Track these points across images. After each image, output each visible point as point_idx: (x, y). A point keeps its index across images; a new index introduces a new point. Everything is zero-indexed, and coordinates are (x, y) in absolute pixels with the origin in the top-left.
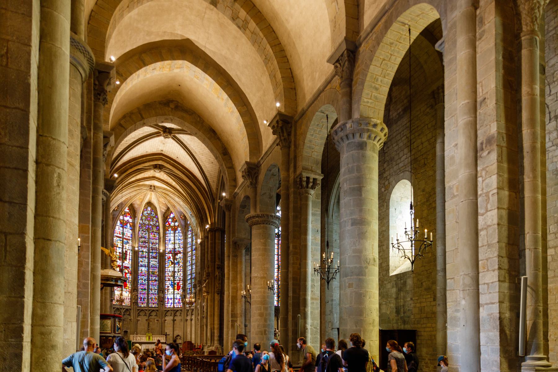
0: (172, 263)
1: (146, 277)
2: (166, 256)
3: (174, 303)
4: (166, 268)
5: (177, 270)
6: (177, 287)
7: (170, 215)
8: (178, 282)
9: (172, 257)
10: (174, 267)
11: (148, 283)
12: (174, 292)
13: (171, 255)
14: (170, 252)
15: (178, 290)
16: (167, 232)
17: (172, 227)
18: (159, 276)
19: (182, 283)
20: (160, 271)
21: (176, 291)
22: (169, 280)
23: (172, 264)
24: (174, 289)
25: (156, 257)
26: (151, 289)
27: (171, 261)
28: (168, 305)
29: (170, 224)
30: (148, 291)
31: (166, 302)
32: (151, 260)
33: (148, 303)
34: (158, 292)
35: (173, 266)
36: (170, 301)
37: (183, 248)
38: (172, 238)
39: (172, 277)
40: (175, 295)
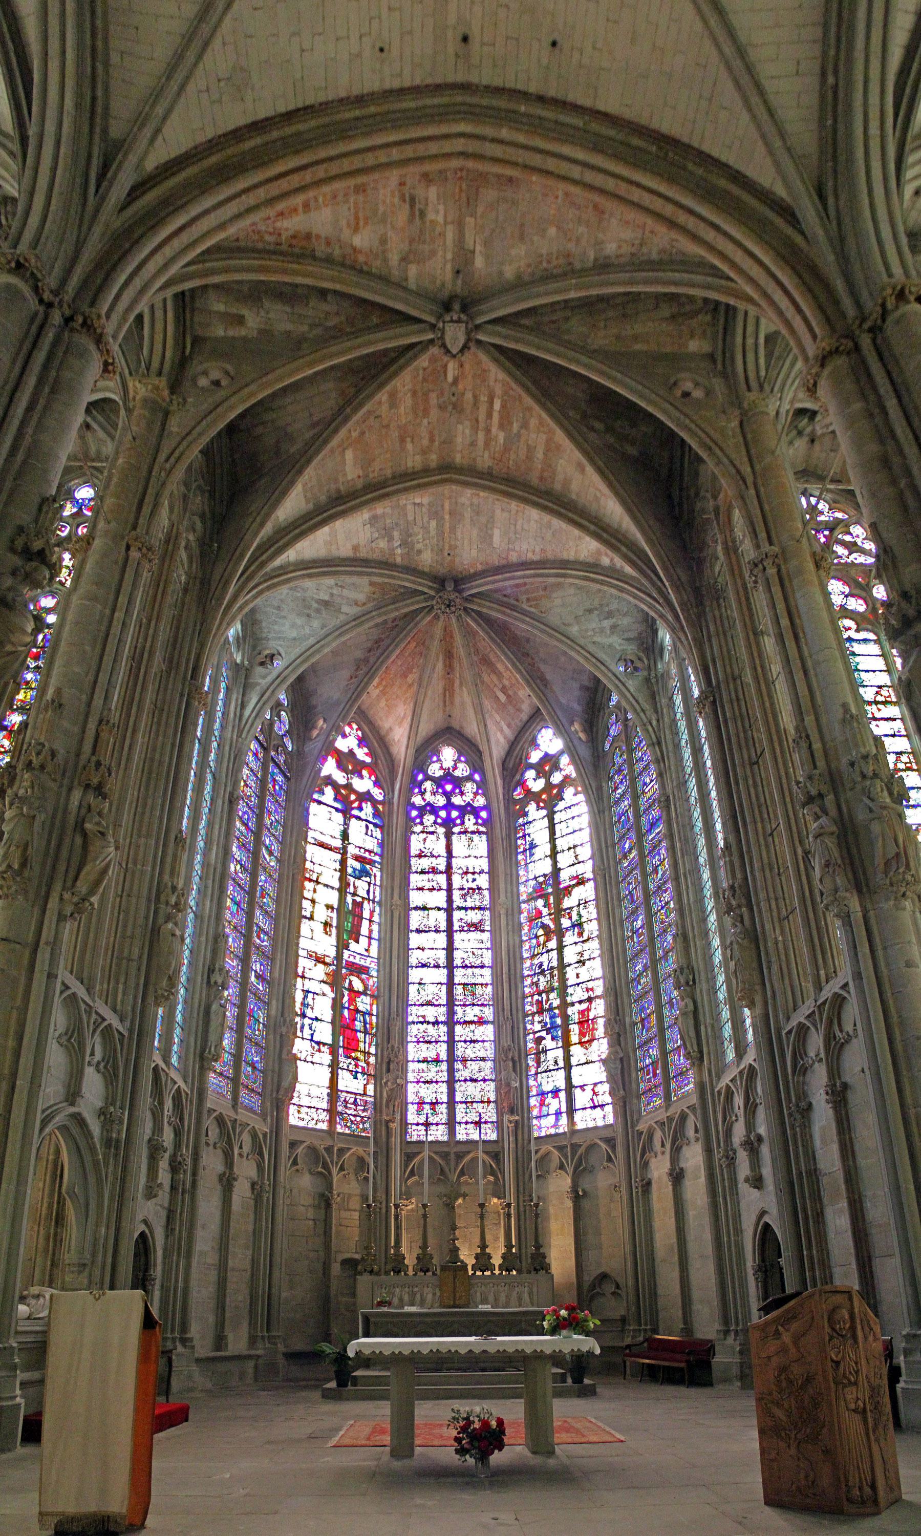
11: (451, 1033)
18: (497, 1002)
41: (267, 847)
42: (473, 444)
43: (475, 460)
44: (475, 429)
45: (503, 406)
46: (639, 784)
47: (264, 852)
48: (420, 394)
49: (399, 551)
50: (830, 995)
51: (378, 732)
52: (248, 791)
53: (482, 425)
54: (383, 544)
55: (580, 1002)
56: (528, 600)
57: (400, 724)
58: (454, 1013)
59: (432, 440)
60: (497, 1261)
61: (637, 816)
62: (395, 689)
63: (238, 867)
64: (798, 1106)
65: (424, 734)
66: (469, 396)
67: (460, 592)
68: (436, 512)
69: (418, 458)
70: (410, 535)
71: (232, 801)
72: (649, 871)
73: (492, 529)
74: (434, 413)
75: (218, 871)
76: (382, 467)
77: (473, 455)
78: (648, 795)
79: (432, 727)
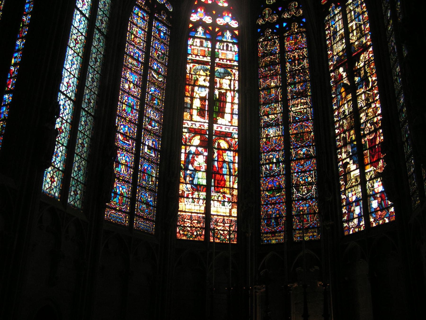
4: (333, 111)
6: (372, 156)
9: (344, 75)
11: (288, 168)
12: (363, 174)
13: (341, 70)
16: (326, 18)
21: (369, 169)
22: (345, 145)
23: (347, 94)
25: (305, 91)
27: (345, 85)
28: (351, 224)
30: (289, 194)
31: (345, 218)
32: (291, 103)
38: (339, 25)
39: (352, 132)
40: (368, 184)
52: (137, 40)
55: (369, 134)
58: (290, 154)
63: (132, 85)
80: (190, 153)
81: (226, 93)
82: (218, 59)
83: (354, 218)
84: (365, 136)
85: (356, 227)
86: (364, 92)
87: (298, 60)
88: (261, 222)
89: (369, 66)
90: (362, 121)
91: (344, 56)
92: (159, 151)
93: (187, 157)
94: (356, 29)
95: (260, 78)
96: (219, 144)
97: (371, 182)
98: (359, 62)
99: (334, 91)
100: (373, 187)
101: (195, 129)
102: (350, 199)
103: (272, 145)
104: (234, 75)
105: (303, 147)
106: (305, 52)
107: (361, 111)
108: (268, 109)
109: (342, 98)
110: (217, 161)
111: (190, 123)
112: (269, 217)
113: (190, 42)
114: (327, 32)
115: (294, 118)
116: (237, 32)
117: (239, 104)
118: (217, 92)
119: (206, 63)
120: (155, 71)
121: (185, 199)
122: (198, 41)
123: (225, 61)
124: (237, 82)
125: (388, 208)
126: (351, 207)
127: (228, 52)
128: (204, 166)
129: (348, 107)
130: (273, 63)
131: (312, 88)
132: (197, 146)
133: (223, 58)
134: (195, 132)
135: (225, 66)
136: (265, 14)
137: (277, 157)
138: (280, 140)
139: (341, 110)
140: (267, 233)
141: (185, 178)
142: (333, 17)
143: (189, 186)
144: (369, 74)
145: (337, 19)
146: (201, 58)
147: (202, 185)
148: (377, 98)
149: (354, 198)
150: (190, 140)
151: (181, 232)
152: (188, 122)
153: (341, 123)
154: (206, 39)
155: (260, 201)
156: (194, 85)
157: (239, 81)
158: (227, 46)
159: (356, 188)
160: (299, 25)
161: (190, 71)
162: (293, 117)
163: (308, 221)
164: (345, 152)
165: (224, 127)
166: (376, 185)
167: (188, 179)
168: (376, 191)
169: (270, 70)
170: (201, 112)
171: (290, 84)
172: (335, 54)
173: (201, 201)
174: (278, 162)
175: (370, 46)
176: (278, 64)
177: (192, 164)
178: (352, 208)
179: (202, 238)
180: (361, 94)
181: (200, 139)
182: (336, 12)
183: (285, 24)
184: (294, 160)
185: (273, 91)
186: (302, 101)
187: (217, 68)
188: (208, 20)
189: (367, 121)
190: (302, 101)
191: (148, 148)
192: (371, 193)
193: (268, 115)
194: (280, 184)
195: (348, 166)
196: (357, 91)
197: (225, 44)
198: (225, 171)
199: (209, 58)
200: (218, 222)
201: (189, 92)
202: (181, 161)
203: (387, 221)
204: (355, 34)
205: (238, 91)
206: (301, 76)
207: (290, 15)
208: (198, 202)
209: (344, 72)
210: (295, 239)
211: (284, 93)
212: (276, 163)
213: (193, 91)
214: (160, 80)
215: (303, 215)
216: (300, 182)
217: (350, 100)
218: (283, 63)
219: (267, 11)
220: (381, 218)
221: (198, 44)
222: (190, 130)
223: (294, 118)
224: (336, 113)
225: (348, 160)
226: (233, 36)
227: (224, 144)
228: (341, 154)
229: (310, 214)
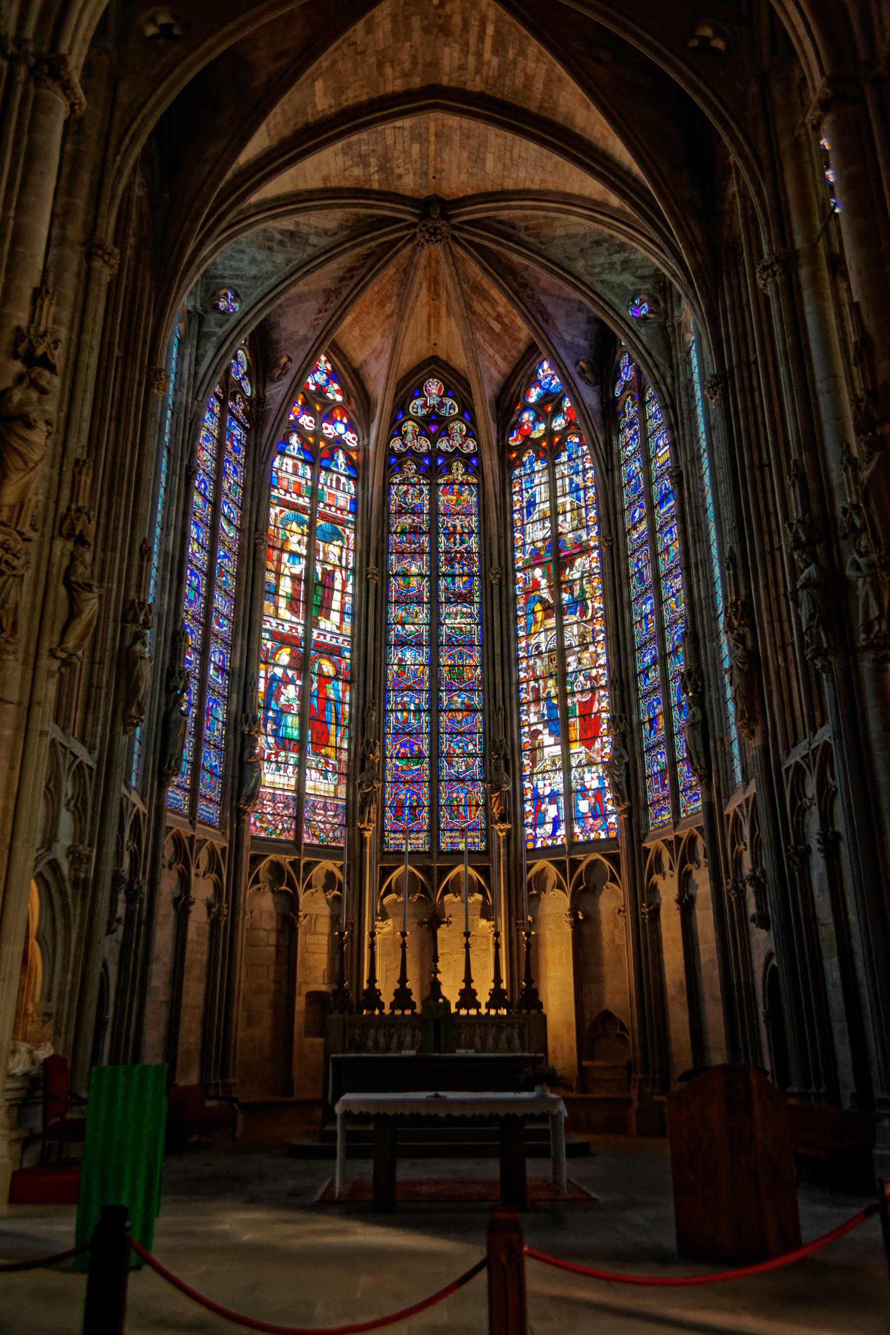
0: (548, 609)
1: (425, 695)
2: (515, 582)
3: (570, 821)
4: (517, 638)
5: (575, 641)
6: (583, 730)
7: (527, 394)
8: (586, 698)
9: (544, 583)
10: (561, 628)
11: (434, 724)
12: (566, 756)
14: (536, 560)
15: (588, 740)
16: (517, 472)
17: (538, 441)
19: (604, 704)
20: (488, 662)
21: (576, 748)
22: (537, 700)
23: (547, 617)
24: (566, 743)
25: (470, 592)
26: (449, 756)
27: (542, 601)
29: (527, 438)
30: (435, 769)
31: (530, 820)
32: (445, 609)
33: (434, 831)
34: (483, 766)
35: (552, 622)
36: (552, 811)
37: (598, 523)
38: (542, 493)
39: (551, 682)
41: (225, 516)
42: (462, 67)
43: (465, 83)
44: (465, 52)
45: (498, 31)
46: (652, 444)
47: (224, 523)
48: (400, 18)
49: (376, 177)
50: (821, 742)
51: (350, 364)
53: (472, 49)
54: (357, 171)
56: (526, 228)
57: (377, 357)
58: (440, 699)
59: (414, 62)
60: (483, 997)
61: (649, 483)
62: (371, 317)
64: (795, 848)
65: (405, 366)
66: (457, 19)
67: (447, 218)
68: (420, 135)
69: (398, 82)
70: (389, 160)
71: (190, 473)
72: (660, 550)
73: (485, 153)
74: (417, 36)
75: (177, 559)
76: (356, 94)
77: (462, 79)
78: (662, 461)
79: (414, 356)
80: (274, 678)
81: (334, 572)
82: (321, 505)
83: (545, 823)
84: (573, 694)
85: (549, 837)
86: (577, 623)
87: (461, 534)
88: (384, 812)
89: (590, 582)
90: (570, 669)
91: (547, 552)
92: (228, 674)
93: (268, 688)
94: (572, 510)
95: (392, 553)
96: (320, 665)
97: (579, 770)
98: (571, 570)
99: (522, 605)
100: (582, 778)
101: (281, 634)
102: (541, 792)
103: (408, 679)
104: (348, 539)
105: (461, 690)
106: (474, 521)
107: (571, 651)
108: (404, 614)
109: (536, 622)
110: (317, 697)
111: (274, 622)
112: (399, 807)
113: (276, 464)
114: (515, 498)
115: (449, 637)
116: (354, 457)
117: (353, 595)
118: (319, 569)
119: (302, 509)
120: (225, 516)
121: (266, 764)
122: (290, 462)
123: (333, 509)
124: (351, 554)
125: (605, 816)
126: (542, 803)
127: (339, 494)
128: (296, 705)
129: (546, 638)
130: (415, 531)
131: (480, 590)
132: (285, 667)
133: (330, 502)
134: (282, 640)
135: (333, 520)
136: (406, 432)
137: (417, 701)
138: (422, 672)
139: (533, 641)
140: (395, 832)
141: (265, 727)
142: (529, 474)
143: (271, 740)
144: (588, 595)
145: (537, 481)
146: (292, 498)
147: (293, 740)
148: (600, 638)
149: (547, 791)
150: (275, 654)
151: (258, 824)
152: (271, 620)
153: (531, 662)
154: (303, 461)
155: (384, 775)
156: (282, 550)
157: (354, 551)
158: (338, 480)
159: (552, 775)
160: (467, 470)
161: (276, 520)
162: (447, 635)
163: (465, 817)
164: (535, 713)
165: (329, 636)
166: (587, 777)
167: (269, 726)
168: (588, 785)
169: (410, 543)
170: (293, 603)
171: (445, 575)
172: (529, 541)
173: (291, 769)
174: (418, 711)
175: (595, 548)
176: (424, 533)
177: (277, 700)
178: (543, 807)
179: (291, 837)
180: (573, 624)
181: (290, 655)
182: (536, 469)
183: (440, 462)
184: (445, 711)
185: (414, 582)
186: (465, 610)
187: (320, 522)
188: (306, 420)
189: (580, 671)
190: (465, 610)
191: (215, 669)
192: (579, 787)
193: (403, 624)
194: (419, 749)
195: (540, 737)
196: (565, 617)
197: (335, 476)
198: (330, 716)
199: (307, 500)
200: (316, 808)
201: (272, 561)
202: (257, 692)
203: (603, 836)
204: (568, 519)
205: (353, 571)
206: (464, 565)
207: (452, 446)
208: (285, 771)
209: (543, 577)
210: (443, 845)
211: (434, 590)
212: (414, 712)
213: (279, 560)
214: (231, 535)
215: (458, 806)
216: (454, 751)
217: (551, 629)
218: (433, 533)
219: (410, 429)
220: (592, 830)
221: (290, 470)
222: (276, 636)
223: (449, 637)
224: (523, 644)
225: (540, 727)
226: (351, 464)
227: (328, 668)
228: (528, 715)
229: (470, 806)
